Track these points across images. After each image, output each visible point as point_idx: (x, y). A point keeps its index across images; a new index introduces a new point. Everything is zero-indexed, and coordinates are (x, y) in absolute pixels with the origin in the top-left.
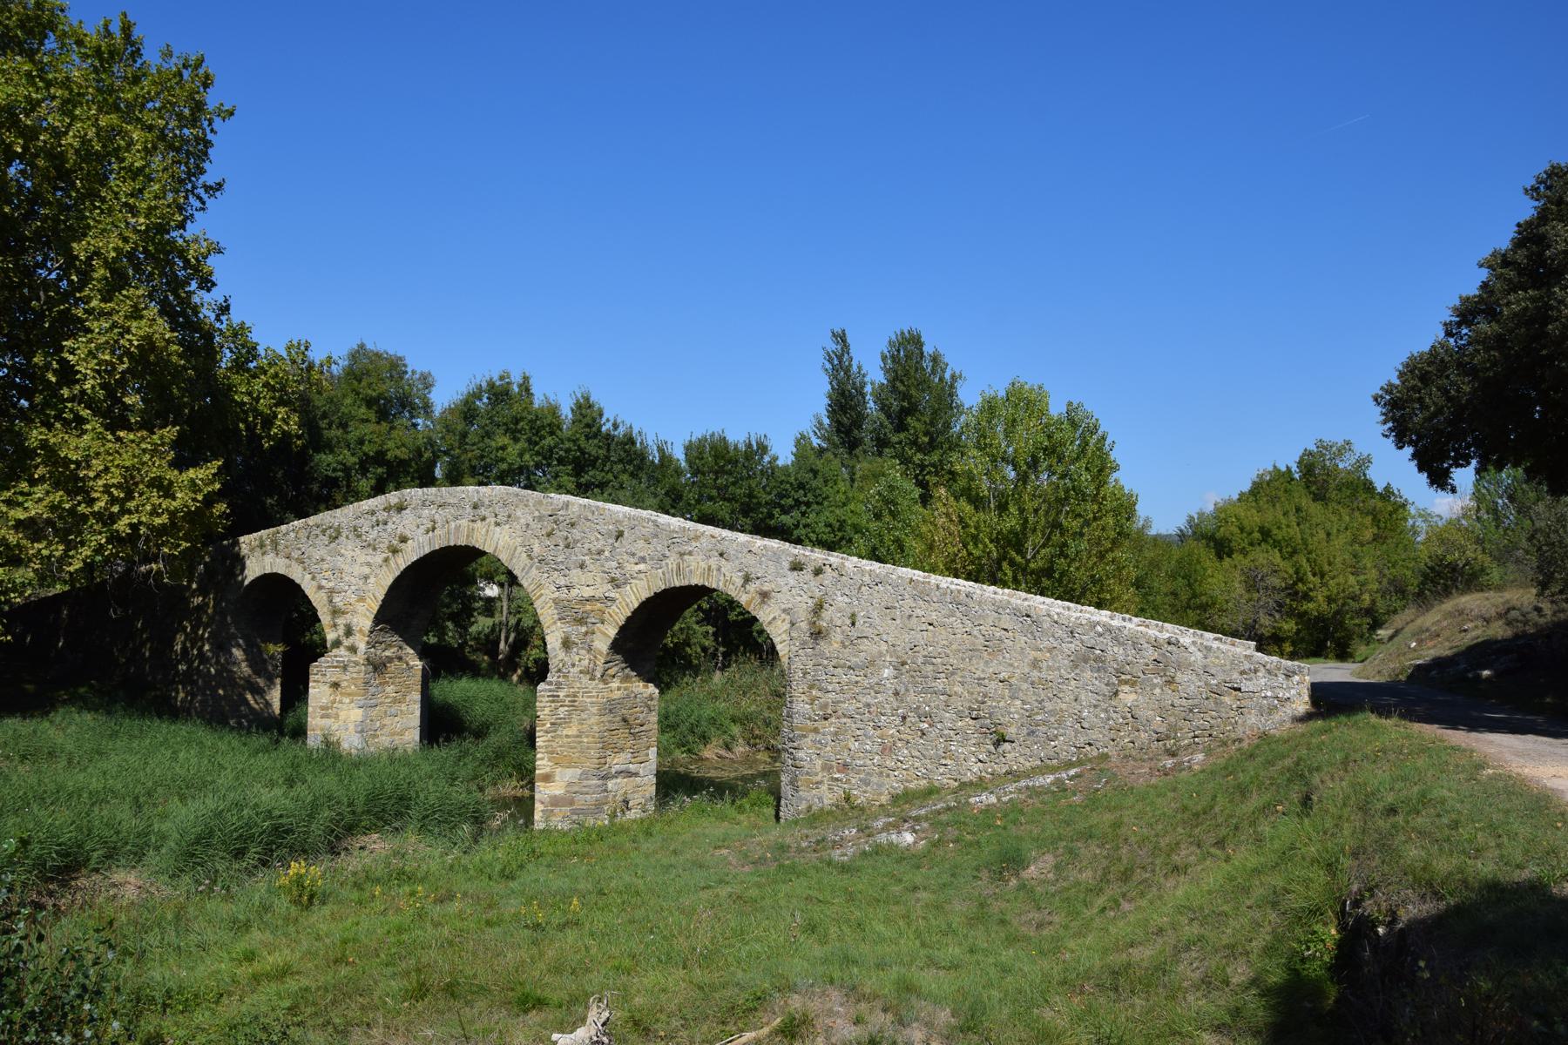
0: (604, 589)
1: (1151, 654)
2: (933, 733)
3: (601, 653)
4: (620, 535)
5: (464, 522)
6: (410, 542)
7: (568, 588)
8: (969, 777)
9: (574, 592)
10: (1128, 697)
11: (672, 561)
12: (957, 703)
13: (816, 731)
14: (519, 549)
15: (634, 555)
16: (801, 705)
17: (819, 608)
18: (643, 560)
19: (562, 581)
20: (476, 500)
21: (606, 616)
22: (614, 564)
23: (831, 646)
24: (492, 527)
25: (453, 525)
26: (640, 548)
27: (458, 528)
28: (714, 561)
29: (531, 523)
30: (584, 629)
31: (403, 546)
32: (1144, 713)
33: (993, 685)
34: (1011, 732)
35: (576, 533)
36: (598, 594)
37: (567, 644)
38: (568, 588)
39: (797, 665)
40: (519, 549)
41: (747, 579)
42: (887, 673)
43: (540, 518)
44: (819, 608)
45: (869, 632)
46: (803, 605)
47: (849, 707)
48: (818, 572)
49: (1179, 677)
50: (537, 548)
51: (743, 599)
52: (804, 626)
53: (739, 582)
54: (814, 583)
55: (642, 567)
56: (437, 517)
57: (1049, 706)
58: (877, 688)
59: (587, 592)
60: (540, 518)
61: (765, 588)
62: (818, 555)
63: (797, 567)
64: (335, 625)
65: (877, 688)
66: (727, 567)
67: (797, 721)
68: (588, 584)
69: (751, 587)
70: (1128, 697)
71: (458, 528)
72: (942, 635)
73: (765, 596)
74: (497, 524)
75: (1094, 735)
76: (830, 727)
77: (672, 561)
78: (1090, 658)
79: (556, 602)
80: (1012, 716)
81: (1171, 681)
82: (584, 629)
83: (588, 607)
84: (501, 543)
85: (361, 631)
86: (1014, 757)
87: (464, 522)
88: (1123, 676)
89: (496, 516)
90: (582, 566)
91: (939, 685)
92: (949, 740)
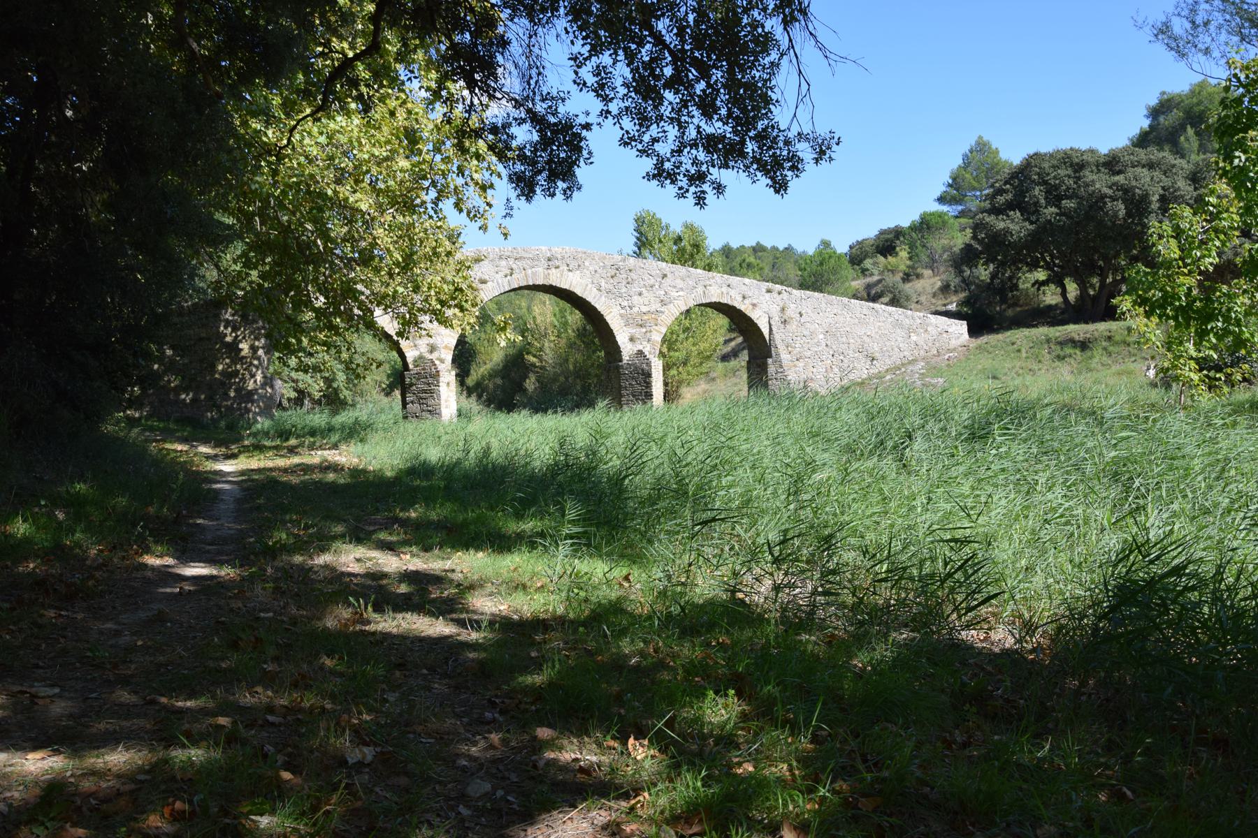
0: (656, 306)
1: (919, 321)
2: (846, 361)
3: (657, 342)
4: (665, 276)
5: (540, 269)
6: (489, 284)
7: (631, 308)
8: (864, 376)
9: (636, 310)
10: (914, 338)
11: (700, 289)
12: (852, 346)
13: (795, 366)
14: (590, 286)
15: (675, 287)
16: (785, 356)
17: (783, 310)
18: (682, 289)
19: (625, 303)
20: (549, 255)
21: (659, 321)
22: (663, 293)
23: (792, 327)
24: (566, 272)
25: (529, 271)
26: (680, 284)
27: (534, 274)
28: (725, 289)
29: (599, 271)
30: (644, 330)
31: (483, 286)
32: (921, 343)
33: (865, 338)
34: (877, 355)
35: (633, 275)
36: (653, 309)
37: (632, 340)
38: (631, 308)
39: (778, 337)
40: (590, 286)
41: (744, 298)
42: (821, 336)
43: (604, 267)
44: (783, 310)
45: (809, 319)
46: (775, 311)
47: (808, 354)
48: (780, 293)
49: (929, 329)
50: (603, 284)
51: (742, 307)
52: (777, 318)
53: (739, 298)
54: (778, 298)
55: (681, 293)
56: (514, 266)
57: (888, 344)
58: (818, 344)
59: (644, 309)
60: (604, 267)
61: (755, 301)
62: (778, 287)
63: (769, 291)
64: (415, 346)
65: (818, 344)
66: (732, 293)
67: (785, 363)
68: (642, 304)
69: (746, 301)
70: (914, 338)
71: (534, 274)
72: (841, 319)
73: (754, 305)
74: (569, 270)
75: (906, 353)
76: (801, 364)
77: (700, 289)
78: (898, 324)
79: (621, 315)
80: (875, 348)
81: (926, 330)
82: (644, 330)
83: (645, 317)
84: (574, 283)
85: (446, 347)
86: (879, 367)
87: (540, 269)
88: (910, 331)
89: (568, 265)
90: (640, 294)
91: (844, 339)
92: (853, 362)
